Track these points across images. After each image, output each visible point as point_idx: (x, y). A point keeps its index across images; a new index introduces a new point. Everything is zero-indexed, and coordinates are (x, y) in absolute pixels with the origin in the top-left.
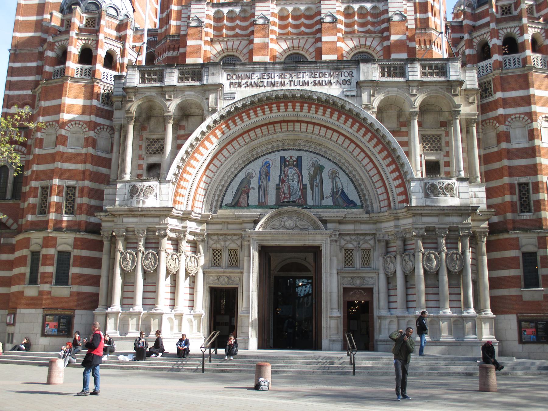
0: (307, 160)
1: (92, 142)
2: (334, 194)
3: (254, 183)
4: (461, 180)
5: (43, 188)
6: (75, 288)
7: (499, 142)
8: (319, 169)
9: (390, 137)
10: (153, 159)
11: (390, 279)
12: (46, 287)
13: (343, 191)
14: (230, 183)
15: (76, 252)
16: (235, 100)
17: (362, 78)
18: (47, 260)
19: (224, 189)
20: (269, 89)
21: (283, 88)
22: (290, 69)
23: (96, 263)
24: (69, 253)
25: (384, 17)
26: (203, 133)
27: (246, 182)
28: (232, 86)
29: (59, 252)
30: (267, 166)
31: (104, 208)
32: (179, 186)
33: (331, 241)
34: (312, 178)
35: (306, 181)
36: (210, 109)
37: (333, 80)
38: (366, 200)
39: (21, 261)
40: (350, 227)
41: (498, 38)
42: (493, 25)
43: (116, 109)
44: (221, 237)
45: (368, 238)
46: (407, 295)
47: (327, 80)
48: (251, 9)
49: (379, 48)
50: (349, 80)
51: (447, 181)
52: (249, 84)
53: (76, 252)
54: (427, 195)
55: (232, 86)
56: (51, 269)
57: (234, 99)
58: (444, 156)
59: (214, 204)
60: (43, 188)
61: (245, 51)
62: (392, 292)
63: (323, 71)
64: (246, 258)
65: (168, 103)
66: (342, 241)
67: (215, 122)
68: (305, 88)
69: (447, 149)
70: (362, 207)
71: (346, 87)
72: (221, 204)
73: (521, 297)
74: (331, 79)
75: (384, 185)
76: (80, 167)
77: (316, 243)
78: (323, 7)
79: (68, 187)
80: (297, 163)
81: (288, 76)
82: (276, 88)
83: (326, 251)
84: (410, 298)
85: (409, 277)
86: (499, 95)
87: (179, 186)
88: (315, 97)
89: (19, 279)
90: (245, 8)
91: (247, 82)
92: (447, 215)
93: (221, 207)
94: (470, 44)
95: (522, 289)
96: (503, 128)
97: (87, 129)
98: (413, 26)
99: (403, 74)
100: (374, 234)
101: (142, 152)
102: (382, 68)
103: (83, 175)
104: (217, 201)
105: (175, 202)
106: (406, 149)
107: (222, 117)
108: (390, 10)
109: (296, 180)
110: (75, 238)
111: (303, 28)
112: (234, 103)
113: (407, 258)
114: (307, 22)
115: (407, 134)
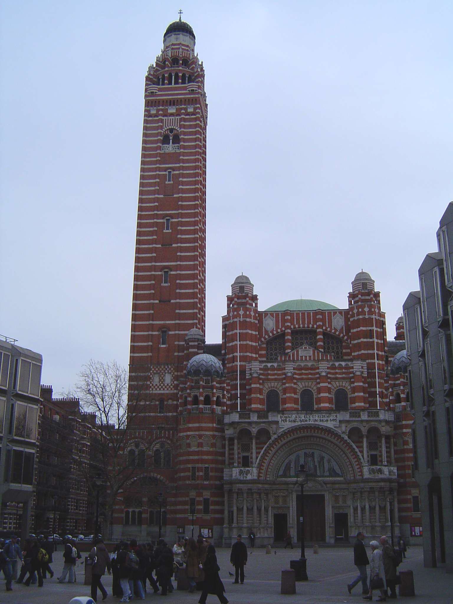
0: (317, 453)
1: (213, 445)
2: (329, 470)
3: (292, 465)
4: (385, 466)
5: (192, 467)
6: (213, 516)
7: (404, 445)
8: (322, 458)
9: (355, 447)
10: (246, 454)
11: (356, 509)
12: (199, 516)
13: (333, 468)
14: (281, 465)
15: (212, 499)
16: (284, 429)
17: (342, 419)
18: (199, 503)
19: (279, 468)
20: (299, 423)
21: (306, 423)
22: (308, 414)
23: (222, 503)
24: (209, 499)
25: (351, 370)
26: (270, 444)
27: (289, 464)
28: (283, 421)
29: (204, 499)
30: (298, 457)
31: (224, 478)
32: (260, 469)
33: (329, 492)
34: (319, 462)
35: (317, 464)
36: (273, 433)
37: (329, 419)
38: (344, 473)
39: (185, 503)
40: (337, 486)
41: (404, 394)
42: (402, 388)
43: (226, 430)
44: (278, 491)
45: (345, 490)
46: (362, 516)
47: (326, 419)
48: (283, 365)
49: (349, 387)
50: (336, 419)
51: (378, 467)
52: (290, 420)
53: (212, 499)
54: (370, 473)
55: (283, 421)
56: (201, 507)
57: (284, 428)
58: (379, 452)
59: (275, 475)
60: (192, 467)
61: (281, 388)
62: (356, 515)
63: (324, 415)
64: (291, 502)
65: (254, 429)
66: (334, 492)
67: (276, 439)
68: (316, 423)
69: (380, 449)
70: (343, 477)
71: (334, 422)
72: (278, 475)
73: (411, 516)
74: (328, 418)
75: (352, 467)
76: (210, 457)
77: (323, 493)
78: (320, 365)
79: (205, 467)
80: (312, 455)
81: (308, 417)
82: (303, 423)
83: (327, 497)
84: (364, 518)
85: (363, 509)
86: (404, 422)
87: (260, 469)
88: (321, 427)
89: (185, 511)
90: (280, 364)
91: (289, 420)
92: (378, 482)
93: (277, 477)
94: (392, 393)
95: (412, 513)
96: (406, 439)
97: (212, 439)
98: (366, 375)
99: (359, 416)
100: (348, 489)
101: (240, 451)
102: (350, 413)
103: (212, 461)
104: (276, 474)
105: (259, 476)
106: (361, 449)
107: (279, 436)
108: (354, 367)
109: (312, 464)
110: (211, 492)
111: (310, 376)
112: (284, 430)
113: (362, 500)
114: (312, 372)
115: (362, 442)
